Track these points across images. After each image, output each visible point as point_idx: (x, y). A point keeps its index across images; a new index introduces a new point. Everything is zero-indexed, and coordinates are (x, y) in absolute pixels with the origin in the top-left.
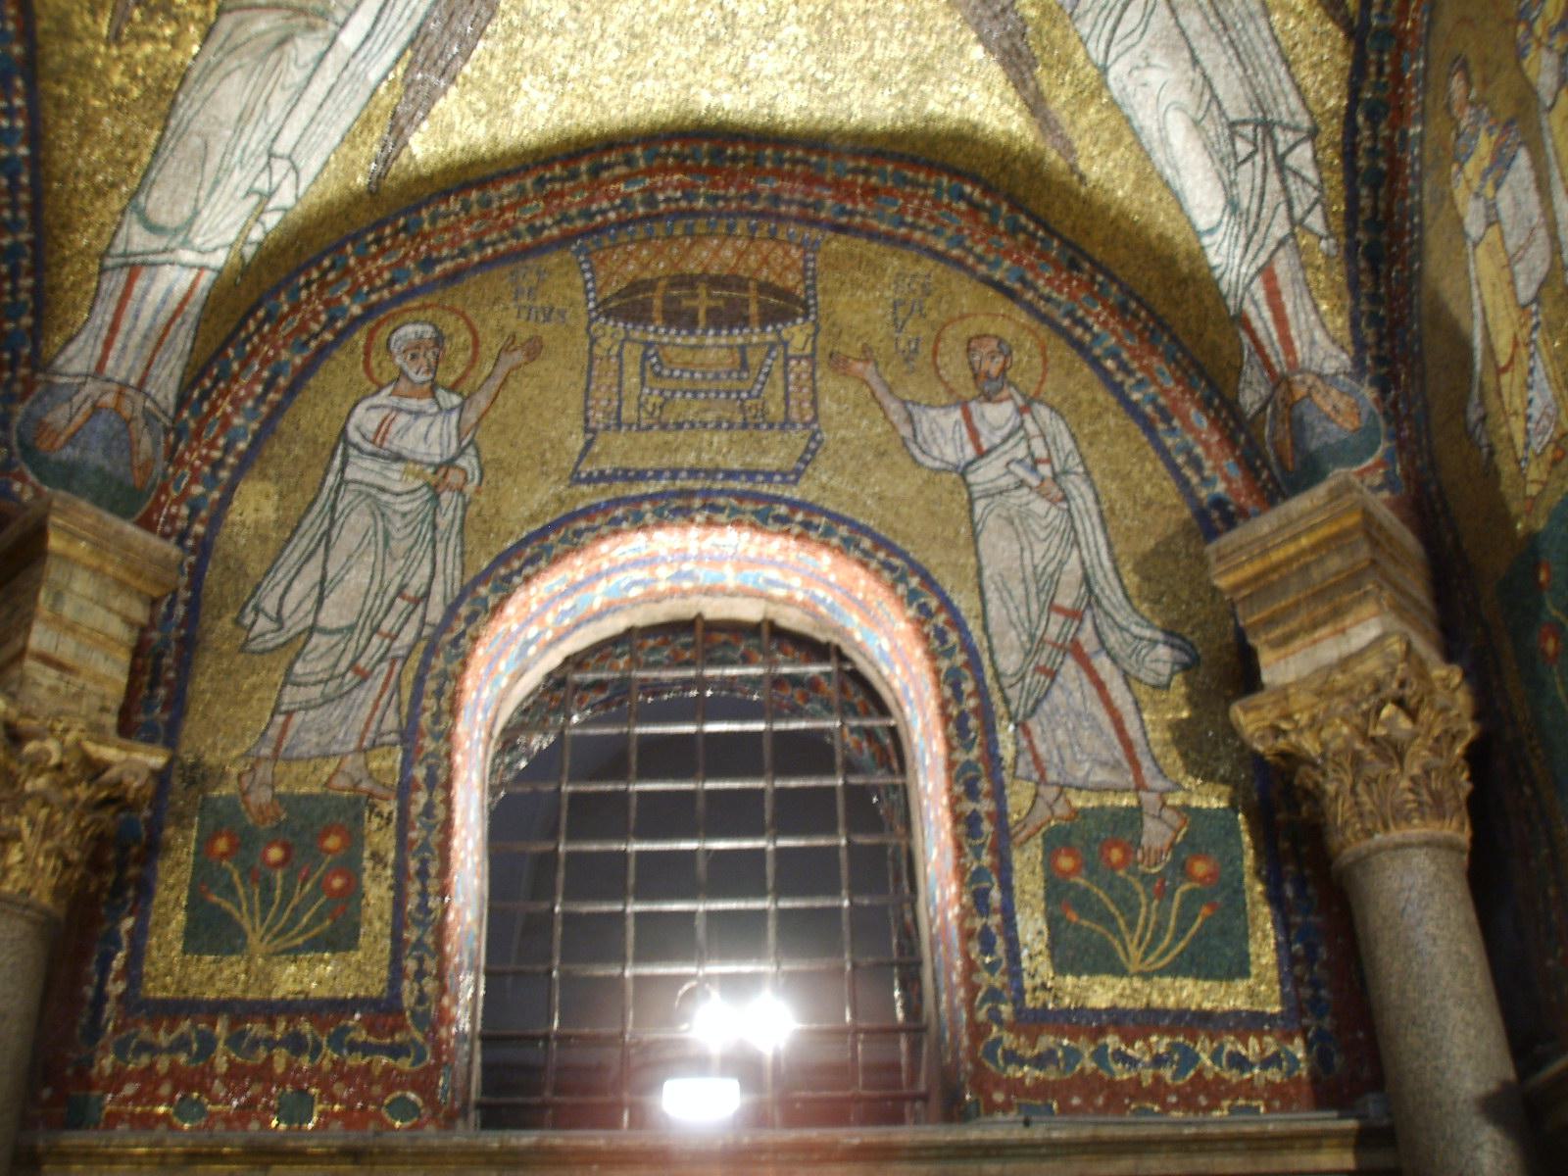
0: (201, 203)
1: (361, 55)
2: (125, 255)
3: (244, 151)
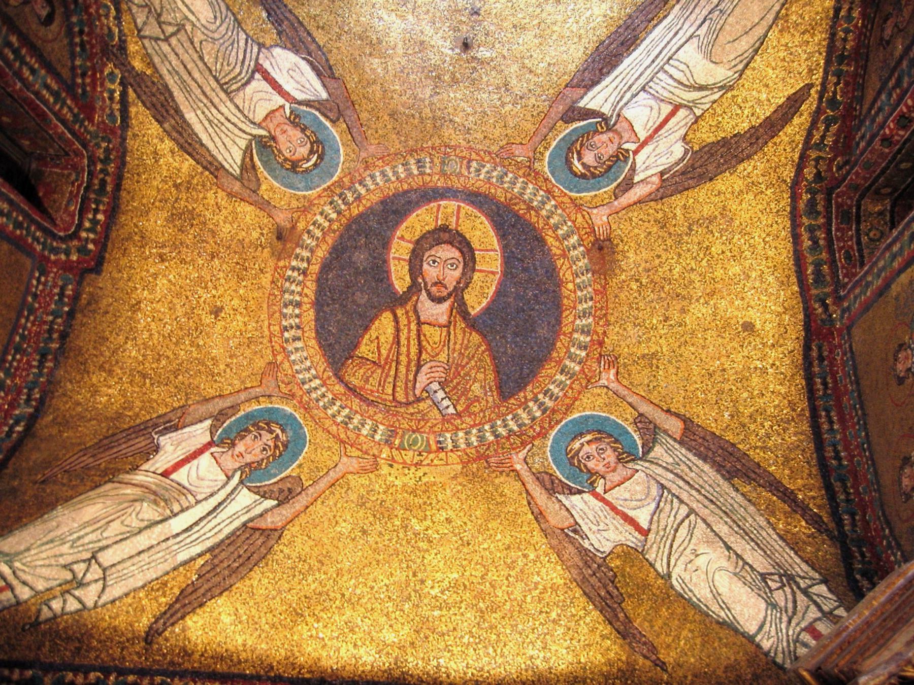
0: (34, 546)
1: (179, 539)
3: (79, 538)
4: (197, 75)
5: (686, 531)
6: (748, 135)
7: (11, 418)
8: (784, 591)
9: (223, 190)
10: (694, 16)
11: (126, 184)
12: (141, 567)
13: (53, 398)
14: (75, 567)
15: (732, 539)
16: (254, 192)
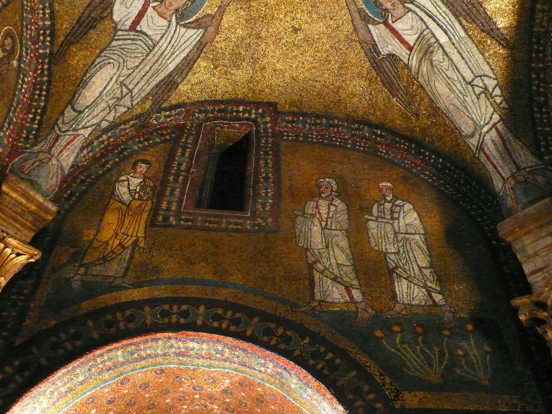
0: (470, 116)
1: (452, 37)
2: (477, 149)
3: (461, 93)
4: (148, 68)
7: (372, 137)
9: (215, 37)
11: (219, 97)
12: (471, 56)
13: (357, 117)
14: (477, 93)
16: (213, 18)
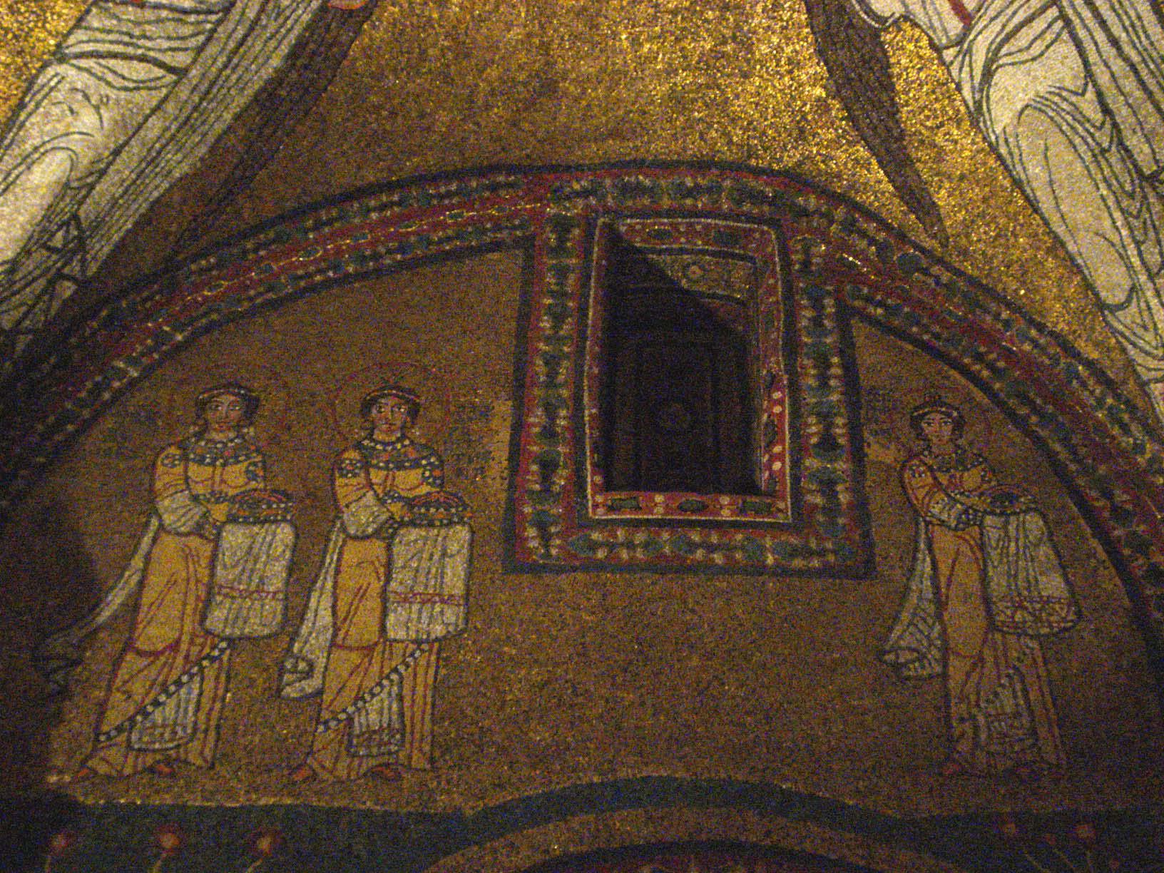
5: (142, 76)
6: (891, 124)
8: (49, 257)
10: (1129, 84)
15: (135, 150)
